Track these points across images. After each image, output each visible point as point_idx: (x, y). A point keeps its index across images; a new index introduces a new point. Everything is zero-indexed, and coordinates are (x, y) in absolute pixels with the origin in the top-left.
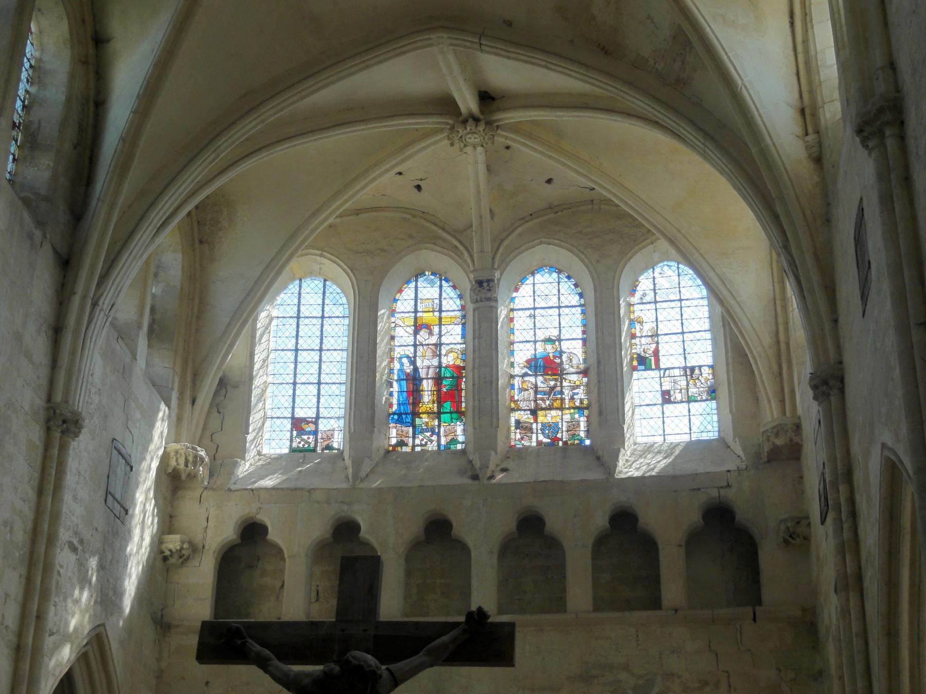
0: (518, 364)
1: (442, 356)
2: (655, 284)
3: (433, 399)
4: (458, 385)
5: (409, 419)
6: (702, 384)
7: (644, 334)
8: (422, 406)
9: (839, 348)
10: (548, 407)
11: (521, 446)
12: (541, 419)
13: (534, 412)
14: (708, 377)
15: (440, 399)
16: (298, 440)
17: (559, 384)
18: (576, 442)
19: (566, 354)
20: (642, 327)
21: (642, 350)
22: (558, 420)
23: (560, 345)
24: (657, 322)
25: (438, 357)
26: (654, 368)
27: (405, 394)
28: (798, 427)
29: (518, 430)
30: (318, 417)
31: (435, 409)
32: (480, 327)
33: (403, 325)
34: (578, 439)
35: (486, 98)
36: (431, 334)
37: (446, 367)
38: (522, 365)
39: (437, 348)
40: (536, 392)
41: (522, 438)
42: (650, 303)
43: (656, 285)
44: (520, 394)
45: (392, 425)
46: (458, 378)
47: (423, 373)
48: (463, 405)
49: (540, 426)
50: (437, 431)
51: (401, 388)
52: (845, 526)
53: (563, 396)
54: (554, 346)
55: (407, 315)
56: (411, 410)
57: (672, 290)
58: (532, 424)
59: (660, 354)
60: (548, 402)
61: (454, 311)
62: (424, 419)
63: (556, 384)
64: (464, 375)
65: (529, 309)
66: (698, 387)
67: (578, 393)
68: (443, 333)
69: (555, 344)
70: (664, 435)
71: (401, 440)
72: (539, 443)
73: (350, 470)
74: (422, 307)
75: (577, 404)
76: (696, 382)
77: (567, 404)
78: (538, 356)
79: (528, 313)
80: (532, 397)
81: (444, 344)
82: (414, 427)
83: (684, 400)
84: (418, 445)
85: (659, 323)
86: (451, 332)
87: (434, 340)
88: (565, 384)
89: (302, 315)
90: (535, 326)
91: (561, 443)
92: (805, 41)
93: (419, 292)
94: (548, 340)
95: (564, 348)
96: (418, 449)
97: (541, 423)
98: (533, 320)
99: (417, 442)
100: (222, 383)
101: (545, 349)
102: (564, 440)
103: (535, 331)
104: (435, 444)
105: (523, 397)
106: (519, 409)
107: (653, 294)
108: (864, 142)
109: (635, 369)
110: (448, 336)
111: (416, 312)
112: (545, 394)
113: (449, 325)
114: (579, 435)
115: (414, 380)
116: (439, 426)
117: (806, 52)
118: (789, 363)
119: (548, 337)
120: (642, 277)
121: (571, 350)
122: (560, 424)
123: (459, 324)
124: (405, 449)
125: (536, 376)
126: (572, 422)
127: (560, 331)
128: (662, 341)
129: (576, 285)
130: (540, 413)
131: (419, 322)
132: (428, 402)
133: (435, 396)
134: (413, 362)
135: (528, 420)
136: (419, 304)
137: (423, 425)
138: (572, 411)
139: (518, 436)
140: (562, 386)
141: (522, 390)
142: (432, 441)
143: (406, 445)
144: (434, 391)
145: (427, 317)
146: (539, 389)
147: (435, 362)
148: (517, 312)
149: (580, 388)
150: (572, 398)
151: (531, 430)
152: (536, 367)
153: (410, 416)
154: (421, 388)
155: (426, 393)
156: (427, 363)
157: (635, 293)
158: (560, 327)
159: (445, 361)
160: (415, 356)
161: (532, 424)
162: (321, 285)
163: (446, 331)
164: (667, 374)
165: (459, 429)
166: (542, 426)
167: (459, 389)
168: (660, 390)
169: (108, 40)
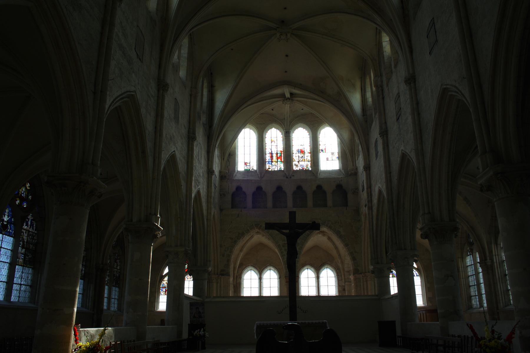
4: (281, 155)
9: (369, 162)
13: (298, 162)
15: (277, 158)
18: (308, 169)
28: (357, 169)
30: (250, 162)
31: (277, 161)
32: (287, 143)
35: (291, 94)
40: (299, 157)
47: (273, 152)
52: (369, 197)
72: (300, 169)
73: (259, 176)
77: (306, 160)
82: (272, 165)
92: (364, 95)
96: (273, 170)
99: (273, 168)
100: (230, 155)
108: (380, 136)
109: (320, 152)
115: (271, 154)
117: (364, 97)
118: (355, 154)
134: (271, 150)
169: (215, 86)
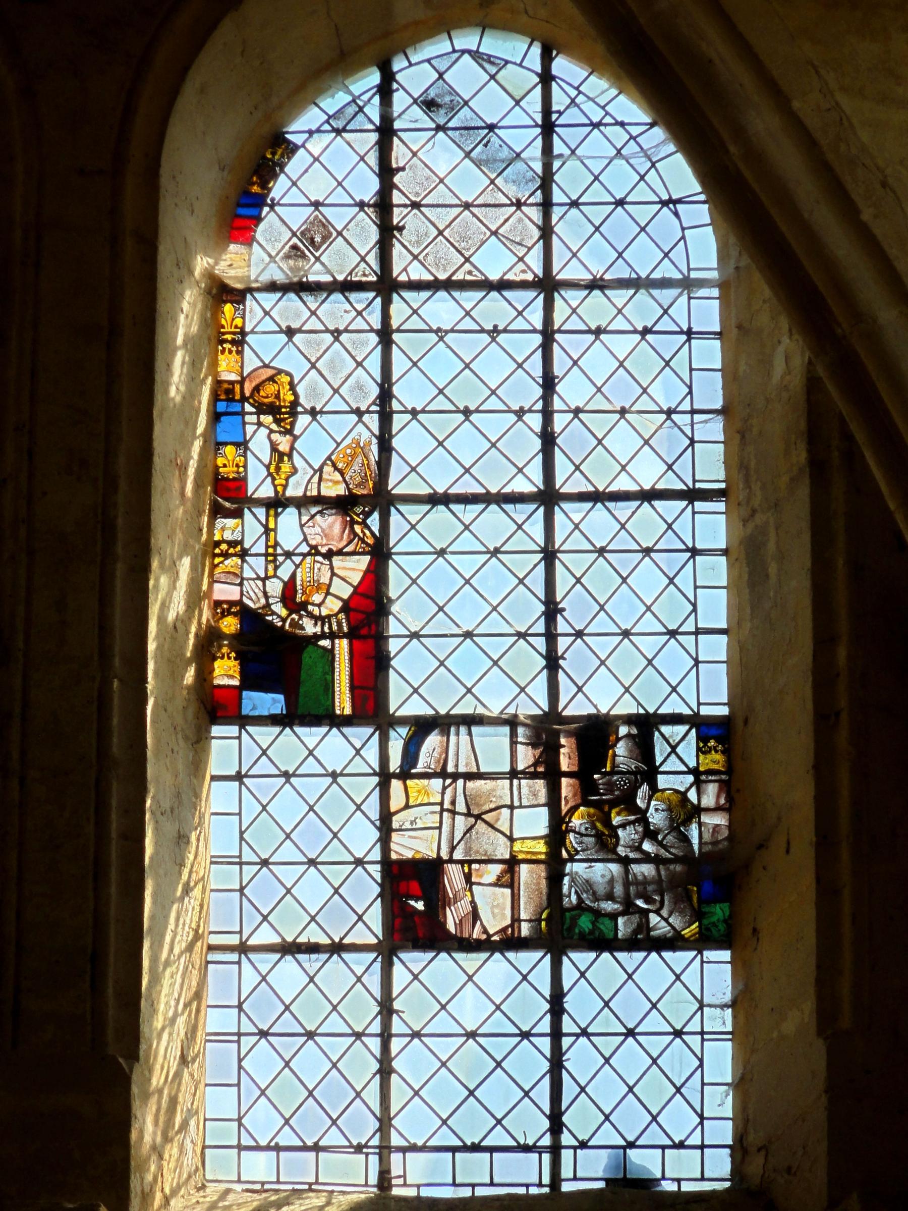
2: (386, 172)
6: (650, 834)
7: (294, 490)
14: (692, 795)
20: (284, 443)
21: (275, 588)
24: (386, 417)
26: (348, 711)
42: (347, 287)
43: (397, 179)
57: (494, 218)
59: (393, 627)
66: (621, 851)
70: (385, 1150)
76: (616, 820)
83: (525, 930)
85: (398, 421)
107: (374, 234)
120: (311, 118)
128: (413, 542)
157: (258, 219)
164: (427, 757)
168: (376, 855)
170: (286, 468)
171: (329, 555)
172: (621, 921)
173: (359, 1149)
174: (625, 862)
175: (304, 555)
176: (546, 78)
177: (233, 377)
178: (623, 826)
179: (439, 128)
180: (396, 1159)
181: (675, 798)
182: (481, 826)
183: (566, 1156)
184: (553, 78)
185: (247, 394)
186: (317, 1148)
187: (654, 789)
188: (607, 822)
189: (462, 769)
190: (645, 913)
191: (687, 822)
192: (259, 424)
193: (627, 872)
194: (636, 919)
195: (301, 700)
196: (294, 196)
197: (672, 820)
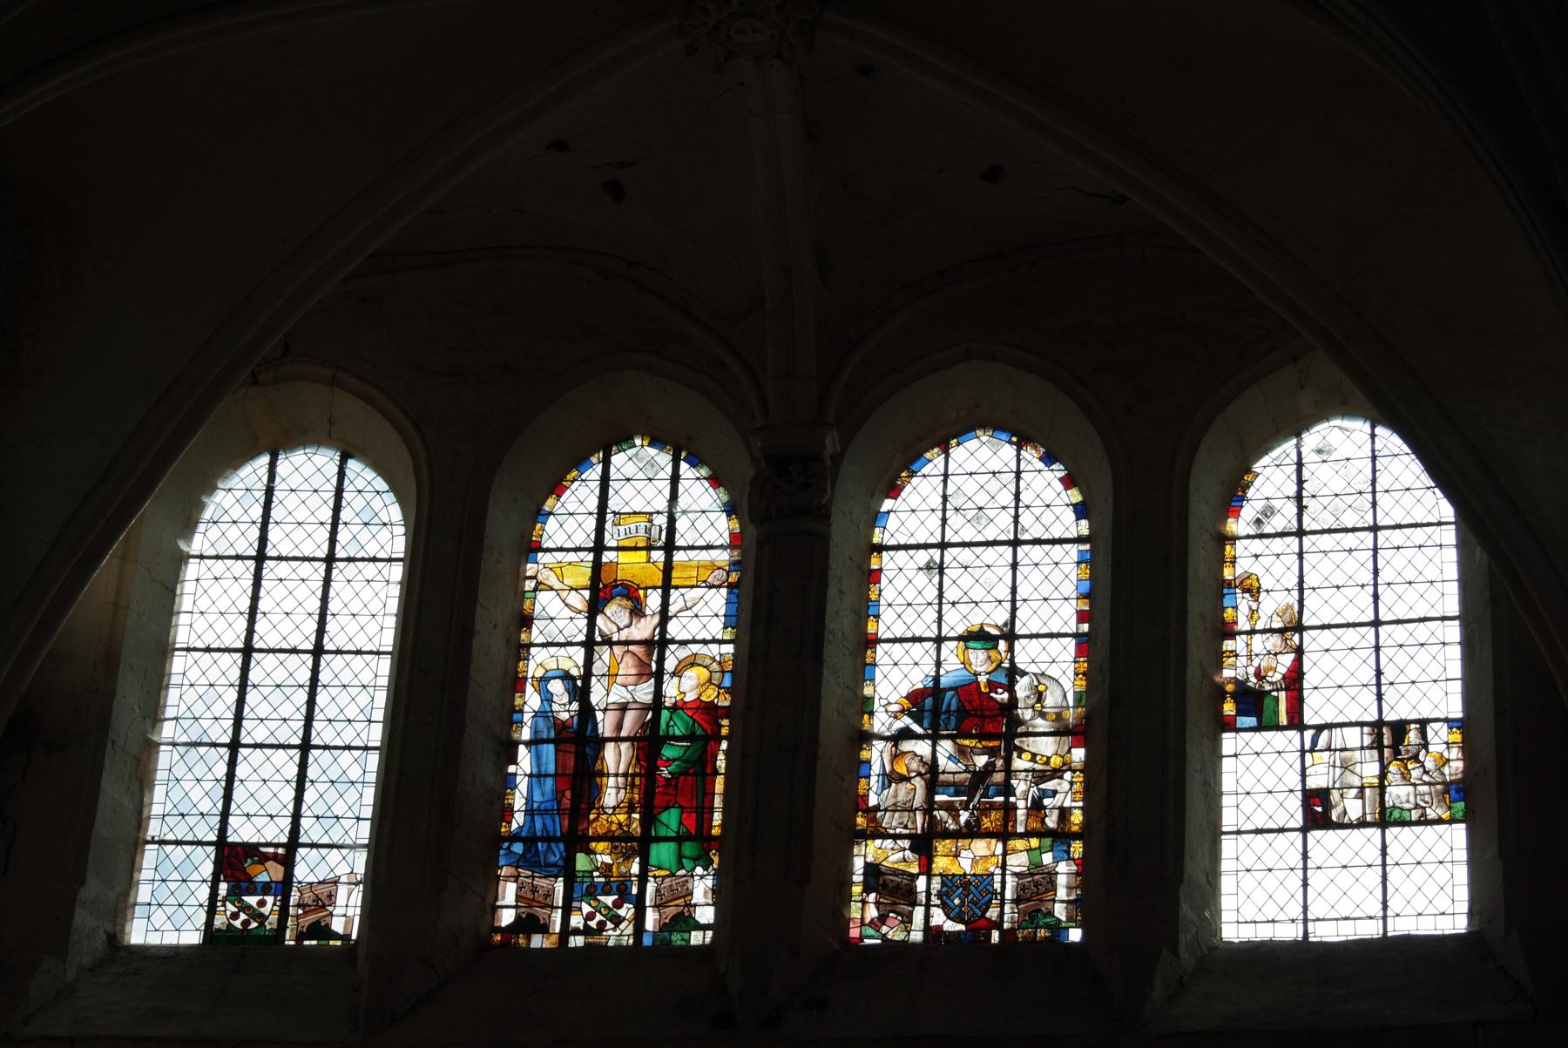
0: (885, 702)
1: (666, 677)
2: (1300, 482)
3: (631, 801)
5: (557, 854)
6: (1426, 772)
7: (1259, 626)
8: (596, 820)
10: (964, 830)
11: (879, 941)
12: (941, 864)
13: (923, 845)
14: (1446, 754)
16: (231, 908)
17: (999, 763)
18: (1042, 933)
19: (1026, 680)
20: (1254, 606)
21: (1251, 670)
22: (992, 869)
23: (1011, 649)
24: (1301, 590)
25: (652, 680)
26: (1285, 723)
27: (549, 782)
29: (872, 897)
30: (293, 843)
31: (636, 827)
33: (557, 585)
34: (1047, 926)
36: (637, 611)
37: (675, 708)
38: (895, 708)
39: (650, 655)
40: (932, 788)
41: (882, 919)
42: (1282, 535)
43: (1305, 485)
44: (885, 792)
45: (504, 872)
46: (702, 742)
48: (717, 818)
49: (936, 884)
50: (635, 891)
51: (539, 766)
53: (1012, 799)
54: (993, 653)
55: (572, 557)
56: (565, 829)
57: (1349, 500)
58: (914, 877)
59: (1306, 684)
60: (964, 816)
61: (709, 547)
62: (598, 856)
63: (993, 764)
64: (724, 731)
65: (926, 546)
66: (1412, 781)
67: (1055, 793)
68: (672, 610)
69: (996, 647)
70: (1306, 921)
71: (529, 915)
72: (931, 931)
74: (616, 536)
75: (1051, 822)
76: (1410, 766)
78: (945, 681)
79: (922, 557)
80: (919, 800)
81: (673, 641)
83: (1369, 818)
84: (576, 932)
85: (1306, 593)
86: (695, 609)
87: (644, 629)
88: (1019, 763)
89: (270, 552)
90: (941, 595)
91: (995, 936)
93: (611, 492)
94: (977, 637)
95: (1021, 661)
96: (577, 941)
97: (940, 875)
98: (936, 580)
99: (576, 921)
101: (966, 663)
102: (1006, 926)
103: (940, 612)
104: (627, 928)
105: (893, 801)
106: (879, 833)
107: (1295, 510)
110: (685, 620)
111: (599, 547)
112: (957, 794)
113: (692, 587)
114: (1050, 913)
116: (643, 879)
119: (976, 629)
120: (1265, 460)
121: (1043, 667)
122: (997, 878)
123: (719, 587)
124: (537, 941)
125: (935, 738)
126: (1032, 875)
127: (1014, 610)
128: (1314, 646)
129: (1068, 482)
130: (942, 846)
131: (606, 578)
132: (614, 808)
133: (636, 791)
134: (580, 690)
135: (902, 867)
136: (608, 525)
137: (596, 874)
138: (1034, 842)
139: (872, 912)
140: (1009, 772)
141: (891, 778)
142: (617, 921)
143: (544, 929)
144: (634, 775)
145: (631, 565)
146: (942, 777)
147: (645, 693)
148: (891, 553)
149: (1061, 778)
150: (1037, 807)
151: (910, 896)
152: (936, 712)
153: (561, 846)
154: (598, 766)
155: (612, 781)
156: (618, 695)
157: (1242, 507)
158: (1014, 601)
159: (671, 690)
160: (587, 674)
161: (914, 877)
162: (333, 469)
163: (681, 604)
164: (1322, 743)
165: (702, 887)
166: (943, 884)
167: (708, 771)
168: (1299, 787)
170: (1255, 616)
171: (1276, 654)
172: (1413, 812)
173: (1293, 921)
174: (1415, 785)
175: (1265, 655)
176: (1373, 436)
177: (1231, 578)
178: (1414, 769)
179: (1324, 461)
180: (1310, 925)
181: (1438, 756)
182: (1347, 772)
183: (1389, 920)
184: (1376, 436)
185: (1237, 584)
186: (1273, 921)
187: (1428, 752)
188: (1406, 768)
189: (1338, 747)
190: (1424, 808)
191: (1444, 765)
192: (1243, 598)
193: (1415, 789)
194: (1420, 811)
195: (1263, 720)
196: (1258, 496)
197: (1436, 765)
